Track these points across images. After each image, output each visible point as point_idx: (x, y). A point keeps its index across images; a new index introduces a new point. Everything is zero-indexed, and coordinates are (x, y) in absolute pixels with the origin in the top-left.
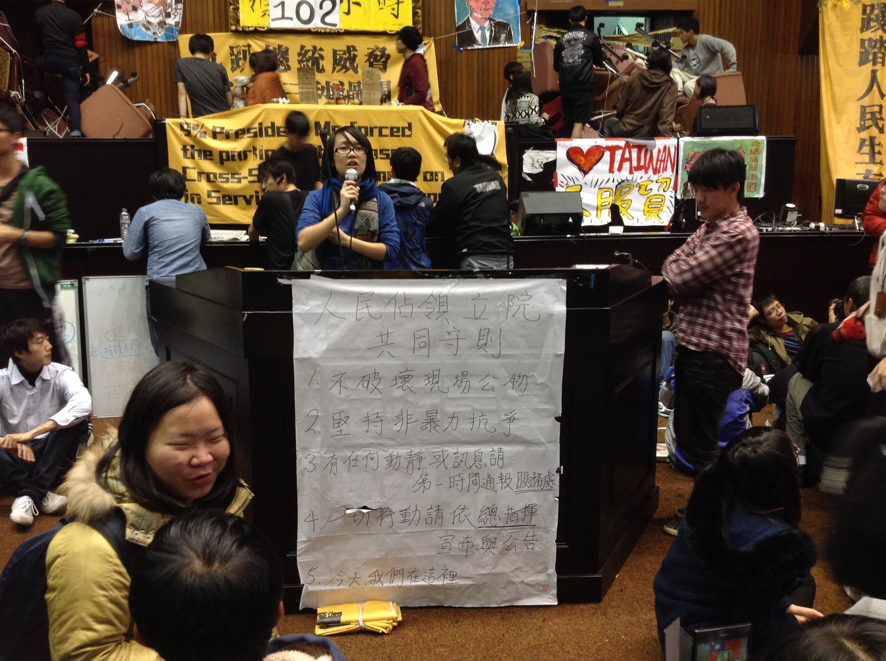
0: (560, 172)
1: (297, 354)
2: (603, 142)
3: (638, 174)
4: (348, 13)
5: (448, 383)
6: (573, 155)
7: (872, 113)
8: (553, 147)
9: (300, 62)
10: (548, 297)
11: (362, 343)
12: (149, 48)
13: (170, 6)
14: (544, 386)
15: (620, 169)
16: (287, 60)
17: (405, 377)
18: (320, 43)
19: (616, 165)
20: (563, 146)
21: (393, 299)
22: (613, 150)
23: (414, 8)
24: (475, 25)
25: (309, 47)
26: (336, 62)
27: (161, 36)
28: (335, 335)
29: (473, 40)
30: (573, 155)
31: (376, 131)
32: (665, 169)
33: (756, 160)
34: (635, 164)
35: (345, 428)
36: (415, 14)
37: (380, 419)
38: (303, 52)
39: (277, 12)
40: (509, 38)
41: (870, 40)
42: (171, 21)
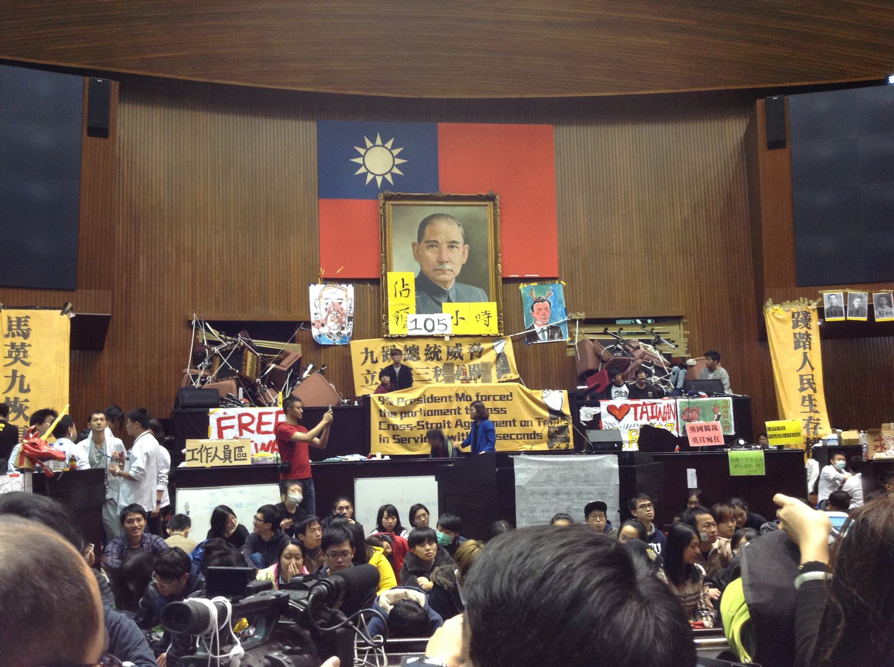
0: (603, 420)
1: (516, 484)
2: (630, 402)
3: (653, 421)
4: (457, 324)
6: (611, 410)
7: (808, 380)
8: (598, 405)
9: (426, 354)
10: (611, 462)
11: (540, 480)
12: (330, 349)
14: (612, 497)
15: (641, 418)
16: (418, 354)
17: (557, 494)
18: (438, 343)
19: (639, 416)
20: (604, 404)
22: (635, 406)
24: (537, 329)
26: (449, 354)
27: (338, 341)
28: (530, 476)
29: (537, 338)
30: (611, 410)
31: (491, 398)
32: (670, 418)
33: (727, 412)
34: (650, 415)
35: (535, 514)
36: (499, 324)
37: (548, 511)
38: (428, 348)
39: (413, 325)
40: (561, 336)
41: (800, 334)
42: (345, 332)
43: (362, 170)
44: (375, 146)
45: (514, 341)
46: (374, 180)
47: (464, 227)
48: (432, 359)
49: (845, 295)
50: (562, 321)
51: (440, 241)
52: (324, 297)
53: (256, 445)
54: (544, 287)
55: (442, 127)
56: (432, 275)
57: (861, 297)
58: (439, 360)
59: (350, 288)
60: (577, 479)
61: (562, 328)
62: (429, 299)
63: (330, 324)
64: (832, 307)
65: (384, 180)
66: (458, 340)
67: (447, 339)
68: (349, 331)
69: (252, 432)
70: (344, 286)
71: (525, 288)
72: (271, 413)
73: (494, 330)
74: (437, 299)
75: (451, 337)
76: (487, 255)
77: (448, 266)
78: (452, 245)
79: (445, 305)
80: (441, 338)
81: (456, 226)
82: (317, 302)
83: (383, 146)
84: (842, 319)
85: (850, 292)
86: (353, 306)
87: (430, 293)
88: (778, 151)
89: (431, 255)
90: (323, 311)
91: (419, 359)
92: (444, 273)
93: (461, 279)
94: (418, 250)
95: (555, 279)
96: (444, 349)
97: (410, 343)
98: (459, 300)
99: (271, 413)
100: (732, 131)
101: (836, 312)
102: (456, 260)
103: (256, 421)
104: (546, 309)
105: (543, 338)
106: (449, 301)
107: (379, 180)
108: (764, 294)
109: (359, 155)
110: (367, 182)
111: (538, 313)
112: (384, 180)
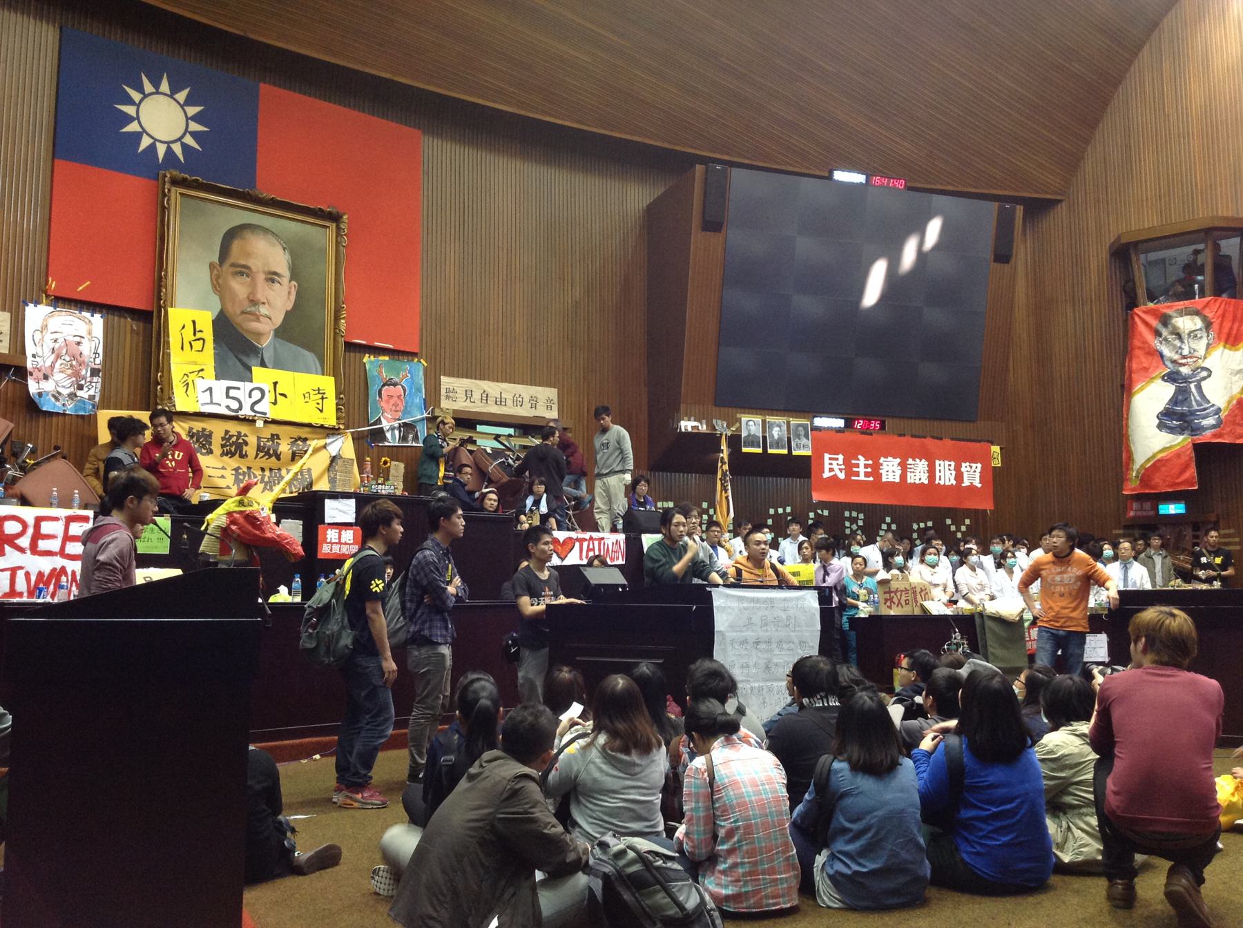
2: (573, 534)
4: (275, 403)
5: (774, 646)
9: (223, 446)
12: (54, 419)
13: (84, 378)
16: (210, 444)
18: (244, 429)
21: (752, 600)
22: (581, 541)
23: (337, 404)
24: (385, 424)
25: (233, 432)
26: (259, 449)
27: (70, 408)
29: (385, 439)
36: (338, 410)
38: (227, 437)
42: (83, 394)
43: (133, 127)
44: (158, 93)
45: (357, 438)
46: (152, 148)
47: (292, 254)
48: (233, 455)
49: (764, 422)
50: (419, 417)
51: (254, 269)
52: (51, 328)
53: (27, 575)
54: (398, 364)
55: (268, 92)
56: (239, 319)
57: (780, 426)
58: (243, 456)
59: (98, 321)
60: (777, 622)
61: (419, 427)
62: (231, 355)
63: (58, 376)
64: (749, 435)
65: (169, 151)
66: (274, 429)
67: (260, 424)
68: (92, 392)
69: (22, 550)
70: (87, 314)
71: (371, 362)
72: (56, 519)
73: (329, 417)
74: (245, 359)
75: (266, 422)
76: (323, 303)
77: (263, 310)
78: (272, 277)
79: (257, 370)
80: (250, 421)
81: (279, 249)
82: (38, 336)
83: (171, 96)
84: (760, 450)
85: (769, 419)
86: (100, 351)
87: (234, 348)
88: (711, 234)
89: (239, 287)
90: (47, 351)
91: (211, 452)
92: (258, 320)
93: (283, 332)
94: (218, 277)
95: (414, 354)
96: (252, 440)
97: (198, 426)
98: (278, 365)
99: (56, 519)
100: (634, 196)
101: (752, 442)
102: (277, 302)
103: (30, 531)
104: (399, 397)
105: (392, 439)
106: (263, 364)
107: (161, 150)
108: (678, 409)
109: (130, 101)
110: (141, 149)
111: (387, 402)
112: (169, 151)
